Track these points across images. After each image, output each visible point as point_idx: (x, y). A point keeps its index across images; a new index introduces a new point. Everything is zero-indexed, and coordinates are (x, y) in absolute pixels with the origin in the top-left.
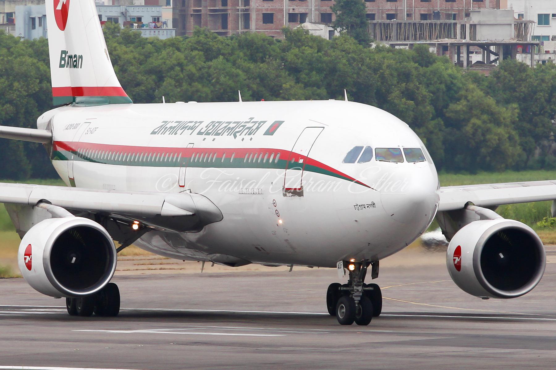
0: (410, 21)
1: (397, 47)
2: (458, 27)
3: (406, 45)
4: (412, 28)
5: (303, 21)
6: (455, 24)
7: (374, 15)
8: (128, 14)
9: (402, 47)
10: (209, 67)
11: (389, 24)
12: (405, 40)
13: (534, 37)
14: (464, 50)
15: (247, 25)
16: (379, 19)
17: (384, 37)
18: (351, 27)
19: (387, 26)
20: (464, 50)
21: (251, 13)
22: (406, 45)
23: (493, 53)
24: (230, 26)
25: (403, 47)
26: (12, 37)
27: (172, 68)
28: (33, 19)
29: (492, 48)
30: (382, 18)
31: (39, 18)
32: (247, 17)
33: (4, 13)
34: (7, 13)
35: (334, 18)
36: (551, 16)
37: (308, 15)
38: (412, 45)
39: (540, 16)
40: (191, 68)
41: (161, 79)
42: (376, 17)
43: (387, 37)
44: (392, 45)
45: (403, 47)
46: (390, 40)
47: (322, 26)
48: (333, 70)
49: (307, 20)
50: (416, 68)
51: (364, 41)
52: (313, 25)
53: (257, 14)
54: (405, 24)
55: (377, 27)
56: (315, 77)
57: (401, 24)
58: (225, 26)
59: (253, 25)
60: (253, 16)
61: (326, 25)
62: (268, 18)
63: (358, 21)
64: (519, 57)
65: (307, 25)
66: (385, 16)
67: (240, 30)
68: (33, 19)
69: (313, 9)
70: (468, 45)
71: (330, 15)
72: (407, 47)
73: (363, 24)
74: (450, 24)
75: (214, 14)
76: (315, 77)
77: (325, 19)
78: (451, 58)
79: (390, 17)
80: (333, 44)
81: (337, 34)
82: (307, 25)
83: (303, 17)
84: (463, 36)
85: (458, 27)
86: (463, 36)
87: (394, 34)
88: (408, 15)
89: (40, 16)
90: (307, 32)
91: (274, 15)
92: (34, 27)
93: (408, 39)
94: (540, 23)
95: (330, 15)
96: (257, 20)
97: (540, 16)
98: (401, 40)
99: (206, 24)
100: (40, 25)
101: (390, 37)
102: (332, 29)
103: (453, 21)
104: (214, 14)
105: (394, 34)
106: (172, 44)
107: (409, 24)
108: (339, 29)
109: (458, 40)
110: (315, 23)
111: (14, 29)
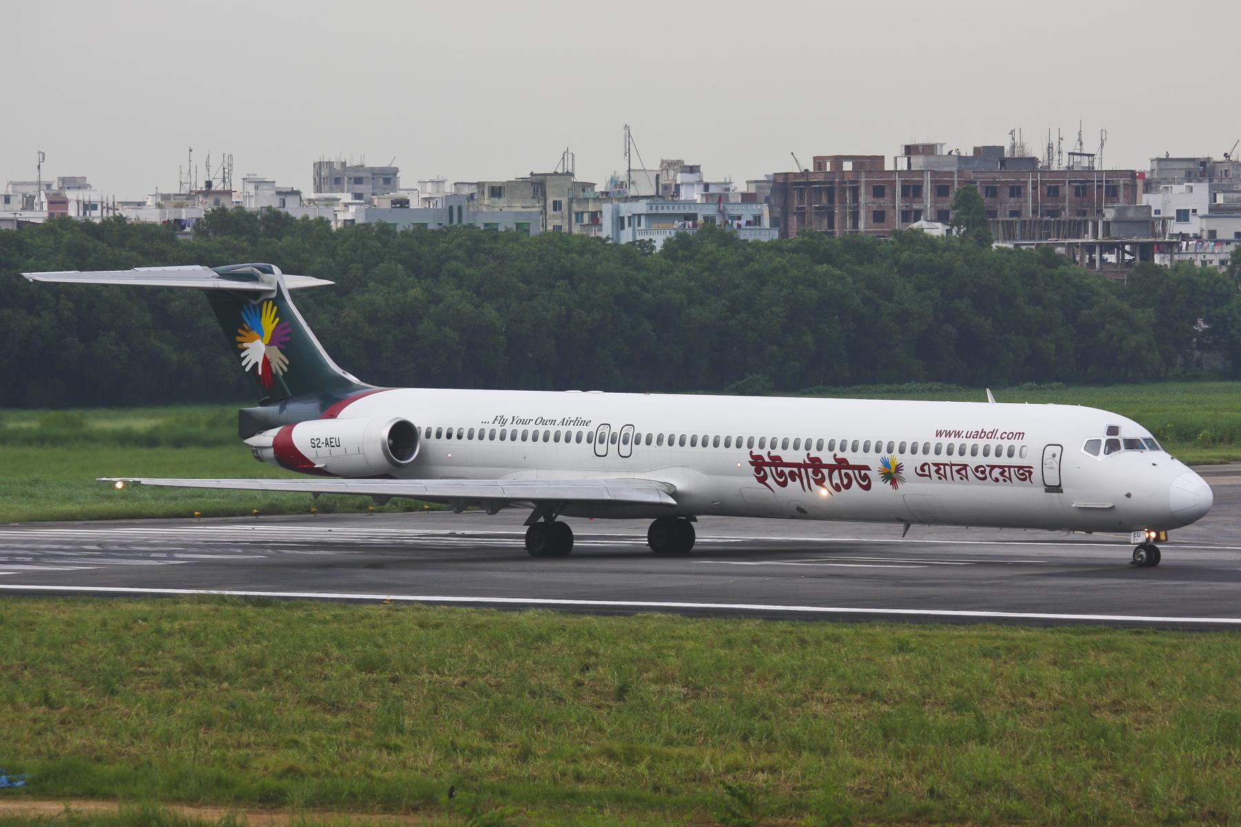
2: (1090, 224)
3: (1033, 244)
5: (917, 219)
6: (1086, 222)
8: (726, 213)
12: (1030, 239)
13: (1172, 236)
14: (1098, 249)
15: (855, 225)
17: (1007, 236)
20: (1098, 249)
22: (1033, 244)
23: (1128, 253)
24: (836, 226)
25: (1027, 245)
26: (599, 238)
28: (622, 219)
29: (1127, 248)
30: (1005, 216)
32: (855, 216)
33: (588, 212)
34: (592, 212)
35: (951, 217)
36: (1191, 211)
37: (923, 212)
38: (1039, 244)
39: (1178, 211)
42: (998, 213)
44: (1016, 245)
46: (1013, 239)
47: (939, 225)
49: (922, 217)
51: (985, 241)
52: (929, 223)
54: (1030, 221)
55: (1000, 225)
57: (1025, 221)
58: (831, 225)
59: (862, 226)
60: (862, 213)
64: (1157, 259)
66: (1008, 213)
68: (622, 219)
69: (929, 206)
70: (1101, 244)
71: (947, 212)
72: (1033, 247)
74: (1080, 222)
75: (820, 212)
77: (941, 216)
78: (1082, 259)
79: (1013, 214)
82: (922, 224)
83: (917, 215)
84: (1095, 235)
85: (1090, 224)
86: (1095, 235)
87: (1018, 232)
88: (1033, 212)
89: (630, 215)
92: (623, 228)
94: (1179, 220)
95: (947, 212)
96: (867, 218)
97: (1178, 211)
98: (1026, 239)
99: (810, 223)
100: (630, 225)
101: (1014, 236)
102: (948, 227)
103: (1084, 218)
104: (820, 212)
105: (1018, 232)
106: (774, 247)
107: (1035, 221)
109: (1089, 239)
110: (931, 221)
111: (601, 230)
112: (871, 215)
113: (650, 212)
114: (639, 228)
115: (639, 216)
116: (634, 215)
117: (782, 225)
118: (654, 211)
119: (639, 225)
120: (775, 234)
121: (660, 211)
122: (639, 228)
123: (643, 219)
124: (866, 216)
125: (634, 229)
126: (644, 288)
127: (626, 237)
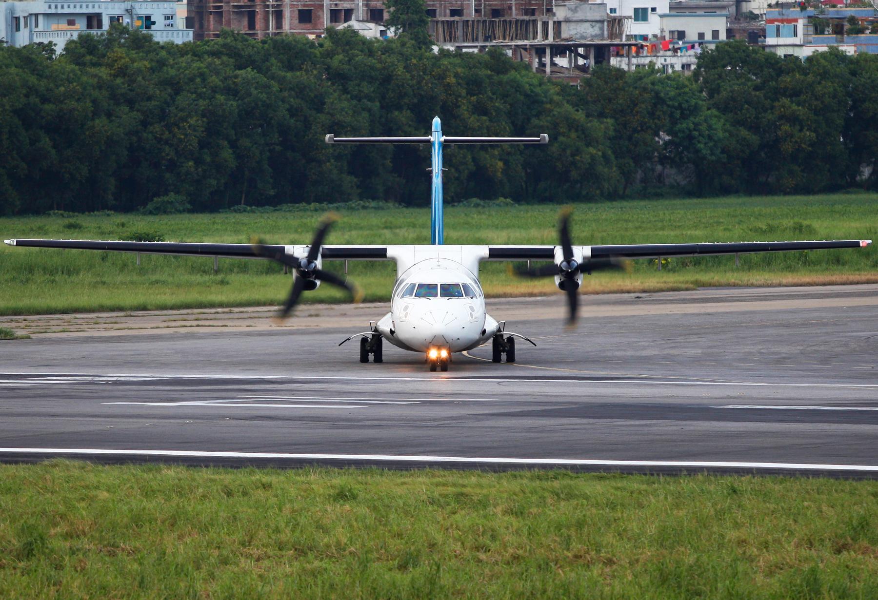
0: (479, 18)
1: (464, 50)
4: (481, 25)
5: (347, 18)
7: (435, 11)
9: (471, 50)
10: (236, 77)
11: (454, 21)
12: (473, 41)
15: (279, 25)
16: (440, 15)
18: (407, 26)
19: (450, 24)
21: (284, 9)
24: (258, 26)
27: (192, 80)
31: (24, 17)
32: (279, 15)
35: (386, 16)
37: (354, 12)
38: (483, 47)
40: (214, 80)
41: (177, 91)
43: (451, 38)
44: (458, 47)
45: (471, 49)
46: (454, 41)
47: (372, 25)
48: (388, 79)
49: (353, 17)
50: (489, 77)
53: (291, 11)
54: (473, 21)
55: (440, 25)
56: (367, 88)
57: (467, 21)
58: (252, 25)
61: (376, 23)
62: (306, 16)
63: (416, 17)
65: (354, 24)
66: (448, 12)
67: (272, 29)
71: (381, 11)
72: (476, 51)
73: (423, 22)
76: (367, 88)
77: (375, 16)
80: (387, 48)
81: (391, 33)
83: (348, 14)
87: (460, 33)
88: (476, 11)
89: (26, 15)
90: (355, 33)
91: (313, 12)
92: (18, 29)
93: (477, 40)
95: (381, 11)
96: (292, 18)
99: (229, 23)
100: (26, 26)
101: (455, 37)
102: (383, 28)
105: (460, 33)
107: (478, 21)
108: (393, 29)
110: (363, 21)
112: (296, 14)
113: (49, 11)
114: (37, 29)
115: (37, 15)
116: (31, 14)
117: (197, 25)
118: (53, 11)
119: (37, 26)
120: (189, 36)
121: (60, 11)
122: (37, 29)
123: (40, 18)
124: (291, 16)
125: (31, 31)
126: (45, 100)
127: (22, 39)
